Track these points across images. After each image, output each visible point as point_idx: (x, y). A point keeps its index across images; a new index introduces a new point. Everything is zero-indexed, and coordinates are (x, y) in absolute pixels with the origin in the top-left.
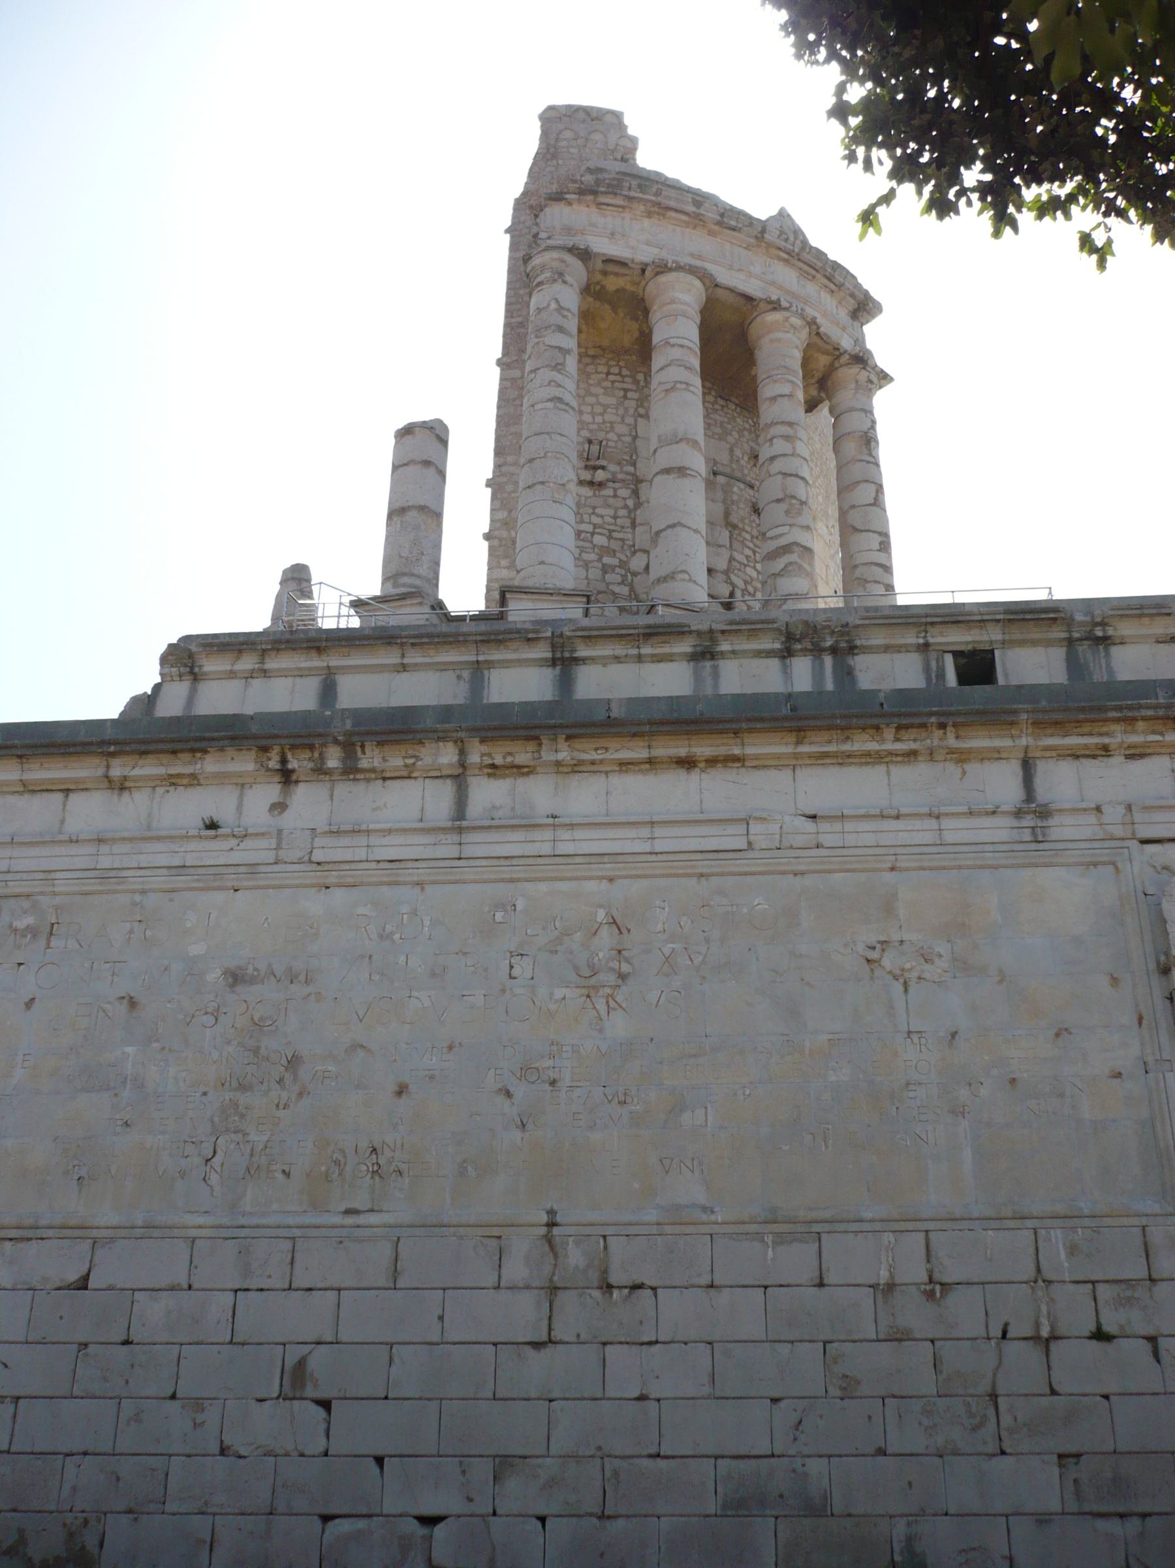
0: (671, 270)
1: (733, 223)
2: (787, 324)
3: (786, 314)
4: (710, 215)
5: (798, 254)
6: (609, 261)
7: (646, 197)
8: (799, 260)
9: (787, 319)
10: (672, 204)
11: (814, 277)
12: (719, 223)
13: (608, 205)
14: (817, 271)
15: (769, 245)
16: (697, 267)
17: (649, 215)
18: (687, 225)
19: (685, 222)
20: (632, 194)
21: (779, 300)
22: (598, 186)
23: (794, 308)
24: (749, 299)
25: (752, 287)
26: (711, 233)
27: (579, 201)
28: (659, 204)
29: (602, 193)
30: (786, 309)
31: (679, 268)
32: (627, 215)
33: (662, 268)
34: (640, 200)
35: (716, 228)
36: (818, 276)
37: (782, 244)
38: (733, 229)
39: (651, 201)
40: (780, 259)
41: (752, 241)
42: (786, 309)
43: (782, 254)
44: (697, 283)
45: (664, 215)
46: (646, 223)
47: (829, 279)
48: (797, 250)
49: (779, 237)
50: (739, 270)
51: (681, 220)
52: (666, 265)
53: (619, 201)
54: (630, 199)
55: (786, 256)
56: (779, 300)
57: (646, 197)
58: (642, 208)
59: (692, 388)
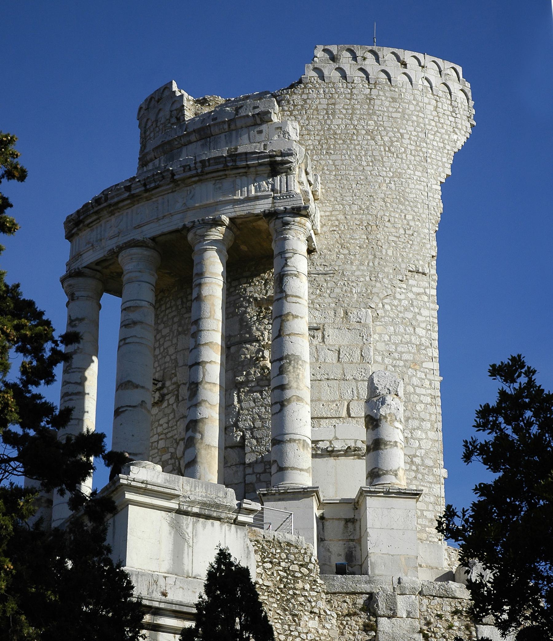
0: (119, 252)
1: (153, 185)
2: (197, 237)
3: (193, 231)
4: (138, 191)
5: (202, 172)
6: (98, 263)
7: (102, 206)
8: (207, 174)
9: (195, 234)
10: (116, 200)
11: (226, 175)
12: (146, 191)
13: (92, 222)
14: (225, 170)
15: (183, 180)
16: (129, 242)
17: (112, 213)
18: (133, 204)
19: (130, 203)
20: (96, 209)
21: (184, 225)
22: (79, 217)
23: (197, 223)
24: (177, 231)
25: (175, 223)
26: (148, 199)
27: (80, 230)
28: (110, 206)
29: (83, 219)
30: (193, 227)
31: (121, 248)
32: (103, 222)
33: (114, 254)
34: (102, 210)
35: (147, 194)
36: (227, 172)
37: (189, 174)
38: (156, 188)
39: (104, 207)
40: (195, 182)
41: (171, 185)
42: (193, 227)
43: (194, 179)
44: (135, 250)
45: (118, 208)
46: (113, 219)
47: (238, 168)
48: (199, 171)
49: (184, 171)
50: (164, 216)
51: (127, 205)
52: (114, 252)
53: (95, 217)
54: (97, 212)
55: (197, 178)
56: (184, 225)
57: (102, 206)
58: (105, 212)
59: (127, 341)
